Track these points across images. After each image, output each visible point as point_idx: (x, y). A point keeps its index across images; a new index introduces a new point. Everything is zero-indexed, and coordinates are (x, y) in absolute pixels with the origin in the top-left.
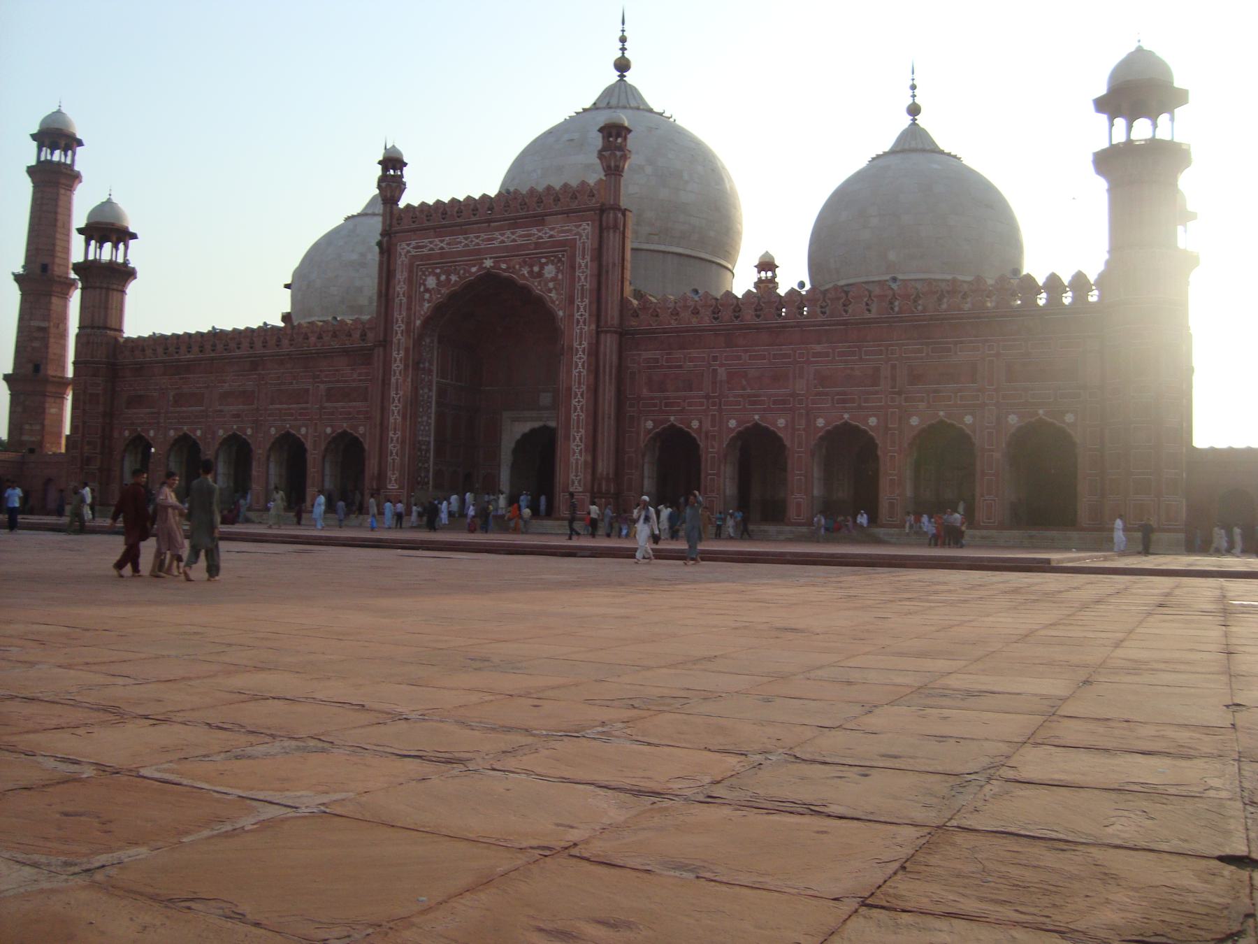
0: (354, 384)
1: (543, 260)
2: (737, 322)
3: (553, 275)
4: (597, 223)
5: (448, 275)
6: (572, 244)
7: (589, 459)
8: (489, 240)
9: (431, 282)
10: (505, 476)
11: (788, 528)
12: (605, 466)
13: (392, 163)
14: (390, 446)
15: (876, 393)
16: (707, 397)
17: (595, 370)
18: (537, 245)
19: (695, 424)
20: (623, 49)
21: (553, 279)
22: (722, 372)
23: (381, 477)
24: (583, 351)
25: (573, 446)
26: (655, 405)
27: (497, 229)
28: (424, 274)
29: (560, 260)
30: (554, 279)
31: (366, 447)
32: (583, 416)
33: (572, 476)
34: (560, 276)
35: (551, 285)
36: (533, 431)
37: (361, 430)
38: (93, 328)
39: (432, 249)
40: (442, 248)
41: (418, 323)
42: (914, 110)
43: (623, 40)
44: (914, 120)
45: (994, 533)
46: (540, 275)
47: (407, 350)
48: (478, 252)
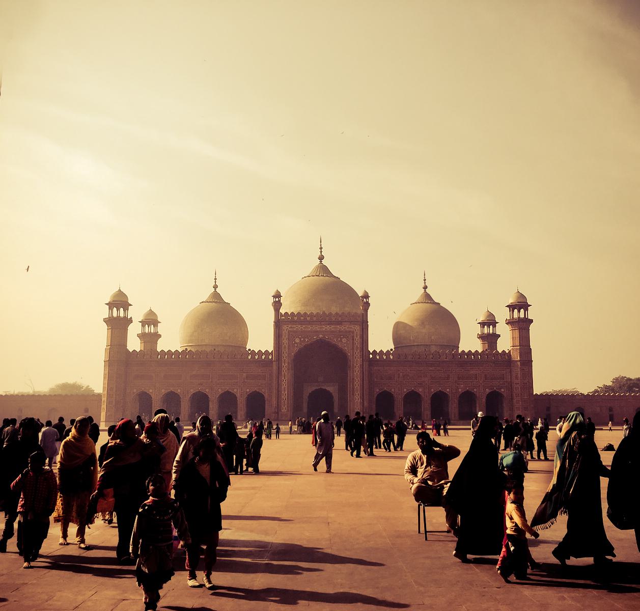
1: (342, 337)
3: (344, 342)
6: (353, 332)
7: (362, 401)
9: (297, 340)
10: (305, 405)
12: (366, 404)
13: (278, 295)
14: (283, 397)
19: (393, 390)
20: (321, 252)
21: (345, 343)
22: (401, 374)
23: (278, 407)
31: (266, 396)
33: (356, 407)
36: (316, 390)
42: (425, 288)
43: (321, 248)
44: (425, 291)
46: (341, 341)
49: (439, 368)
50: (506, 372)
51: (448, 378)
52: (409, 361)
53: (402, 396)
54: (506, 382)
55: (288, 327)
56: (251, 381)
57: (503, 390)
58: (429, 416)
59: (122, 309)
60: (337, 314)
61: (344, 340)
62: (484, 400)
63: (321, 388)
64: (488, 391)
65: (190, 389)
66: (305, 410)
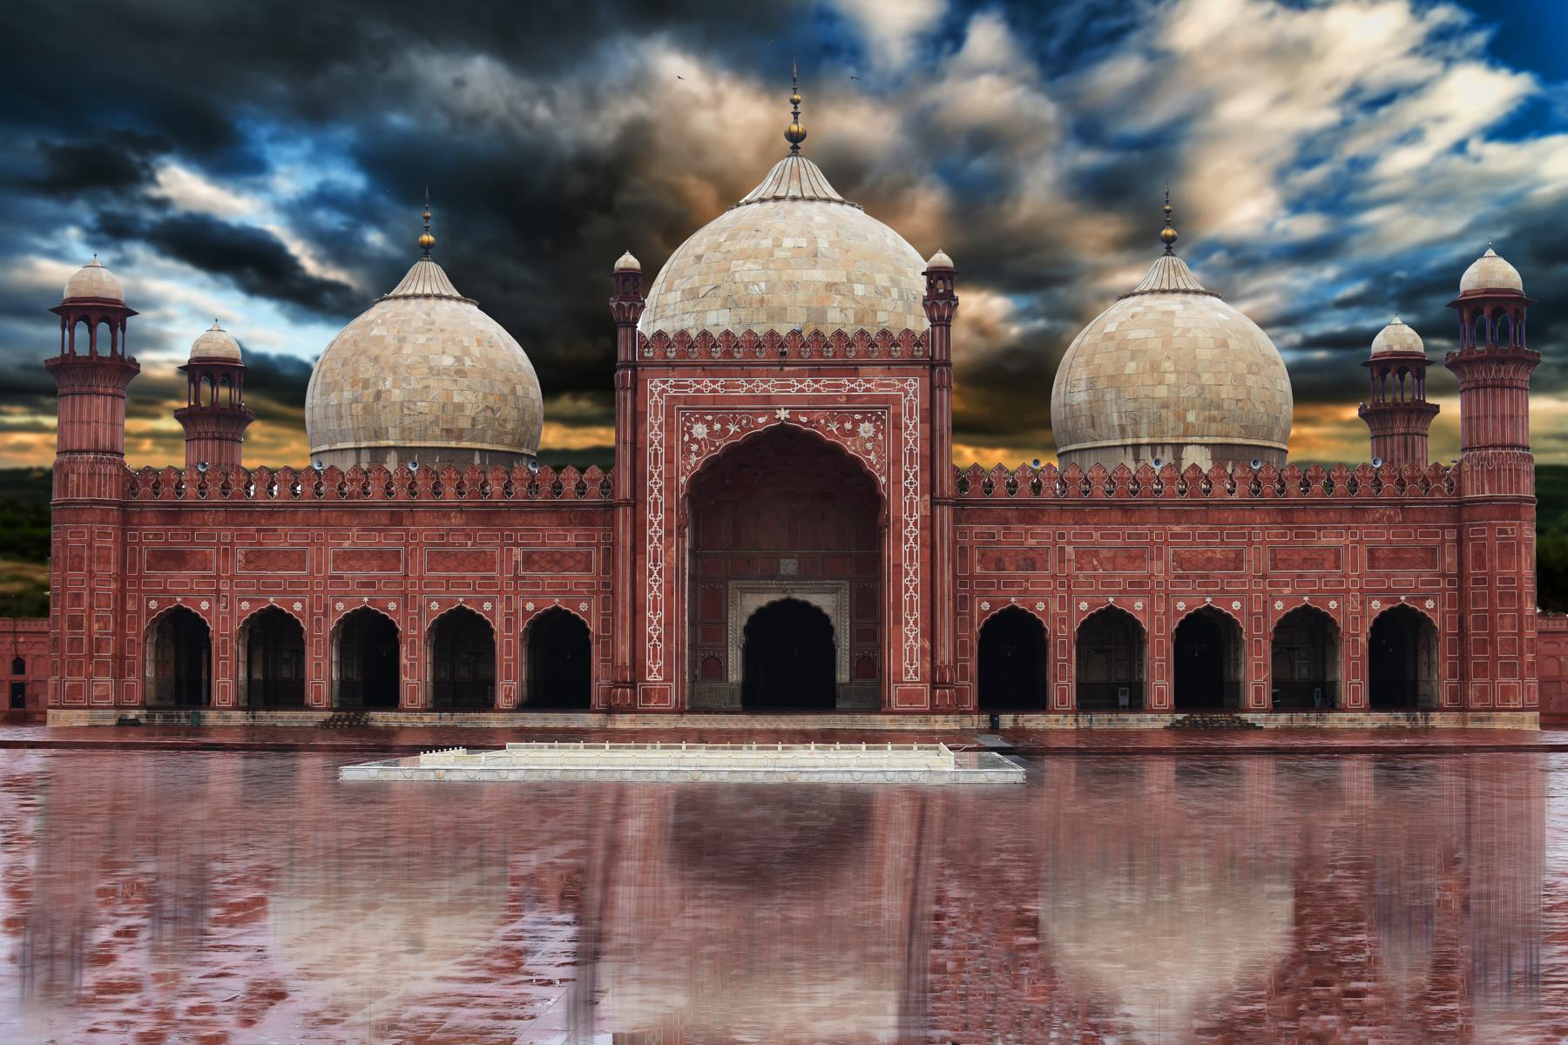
0: (573, 549)
1: (857, 417)
2: (1086, 498)
3: (871, 434)
4: (927, 381)
5: (724, 422)
6: (896, 400)
7: (927, 645)
8: (782, 386)
9: (700, 430)
11: (1149, 716)
12: (945, 655)
15: (1242, 576)
16: (1054, 576)
17: (931, 547)
18: (849, 399)
19: (1040, 606)
21: (869, 440)
22: (1070, 549)
23: (637, 665)
24: (915, 524)
25: (904, 630)
26: (992, 584)
27: (793, 374)
28: (688, 419)
29: (879, 418)
30: (873, 439)
32: (917, 597)
34: (880, 437)
35: (869, 446)
36: (772, 605)
37: (583, 606)
38: (96, 452)
39: (698, 391)
40: (714, 391)
41: (683, 480)
45: (1361, 715)
46: (853, 433)
47: (669, 510)
48: (768, 399)
49: (1204, 529)
50: (1443, 541)
51: (1237, 562)
52: (1098, 503)
53: (1070, 627)
54: (1444, 575)
55: (664, 382)
56: (540, 574)
57: (1429, 604)
58: (1169, 699)
59: (103, 328)
60: (839, 334)
61: (866, 429)
62: (1363, 640)
63: (790, 603)
64: (1377, 605)
65: (335, 602)
66: (735, 674)
